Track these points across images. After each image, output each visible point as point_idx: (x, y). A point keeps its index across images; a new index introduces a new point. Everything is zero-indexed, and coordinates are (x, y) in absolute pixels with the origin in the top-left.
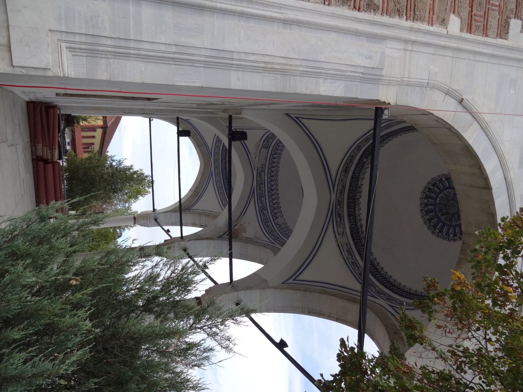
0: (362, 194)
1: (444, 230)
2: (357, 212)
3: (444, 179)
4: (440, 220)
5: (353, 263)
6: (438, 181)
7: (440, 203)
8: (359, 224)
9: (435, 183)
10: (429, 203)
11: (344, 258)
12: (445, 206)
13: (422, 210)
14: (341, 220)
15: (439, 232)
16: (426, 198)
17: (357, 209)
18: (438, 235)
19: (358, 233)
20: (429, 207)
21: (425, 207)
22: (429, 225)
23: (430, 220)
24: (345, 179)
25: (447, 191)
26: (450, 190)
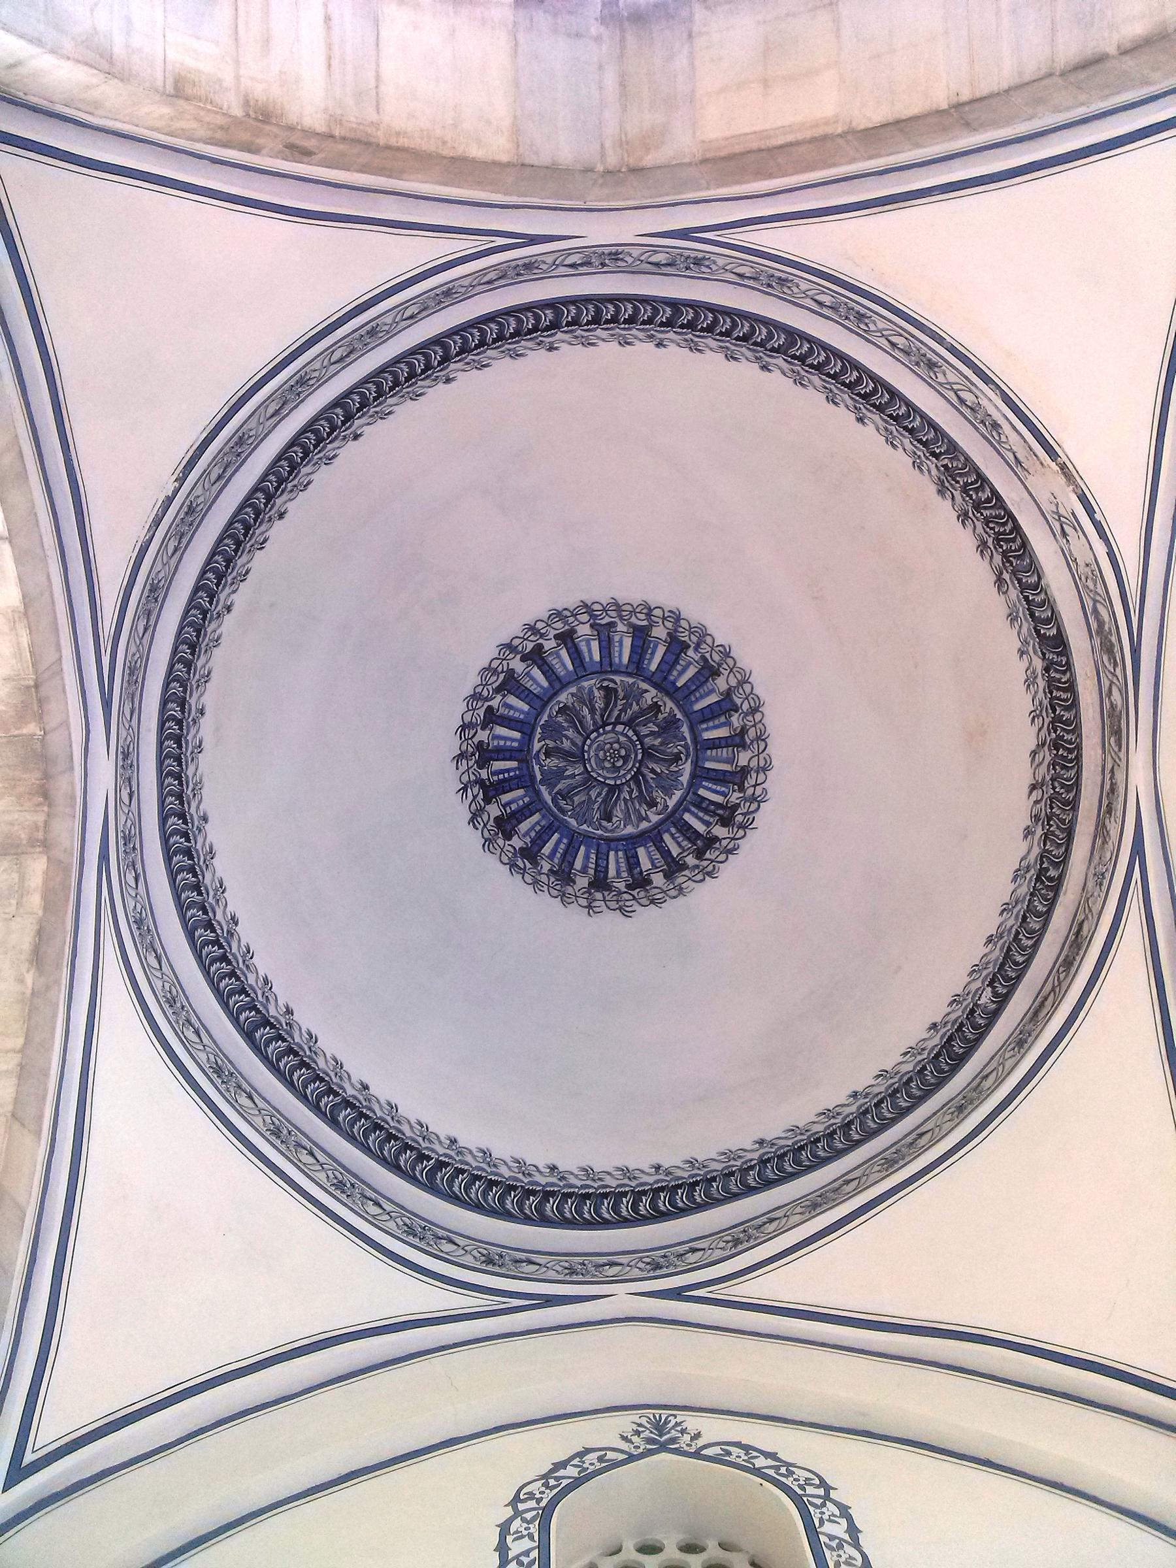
0: (1028, 780)
1: (628, 642)
2: (1038, 664)
3: (658, 879)
4: (662, 682)
5: (931, 365)
6: (684, 867)
7: (677, 758)
8: (1014, 593)
9: (700, 855)
10: (725, 753)
11: (987, 380)
12: (648, 753)
13: (754, 710)
14: (1095, 611)
15: (649, 627)
16: (745, 771)
17: (1041, 683)
18: (649, 615)
19: (997, 540)
20: (723, 732)
21: (744, 731)
22: (705, 648)
23: (709, 671)
24: (1090, 884)
25: (644, 825)
26: (630, 830)
